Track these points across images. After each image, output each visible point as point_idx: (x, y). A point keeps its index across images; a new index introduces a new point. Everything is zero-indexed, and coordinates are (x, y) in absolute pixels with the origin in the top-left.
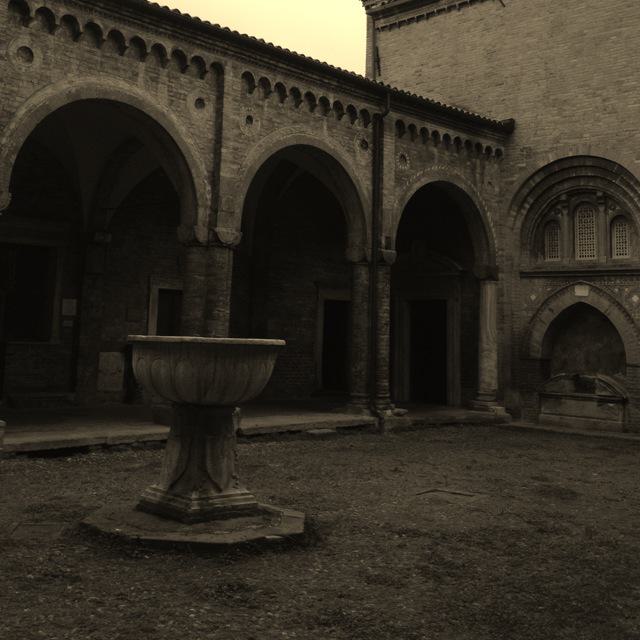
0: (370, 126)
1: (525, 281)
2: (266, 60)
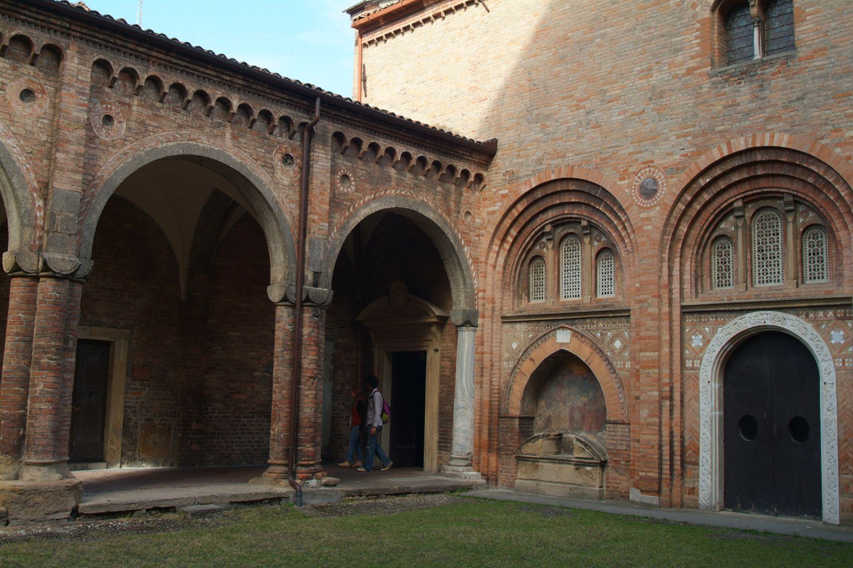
0: (297, 136)
1: (507, 326)
2: (130, 46)
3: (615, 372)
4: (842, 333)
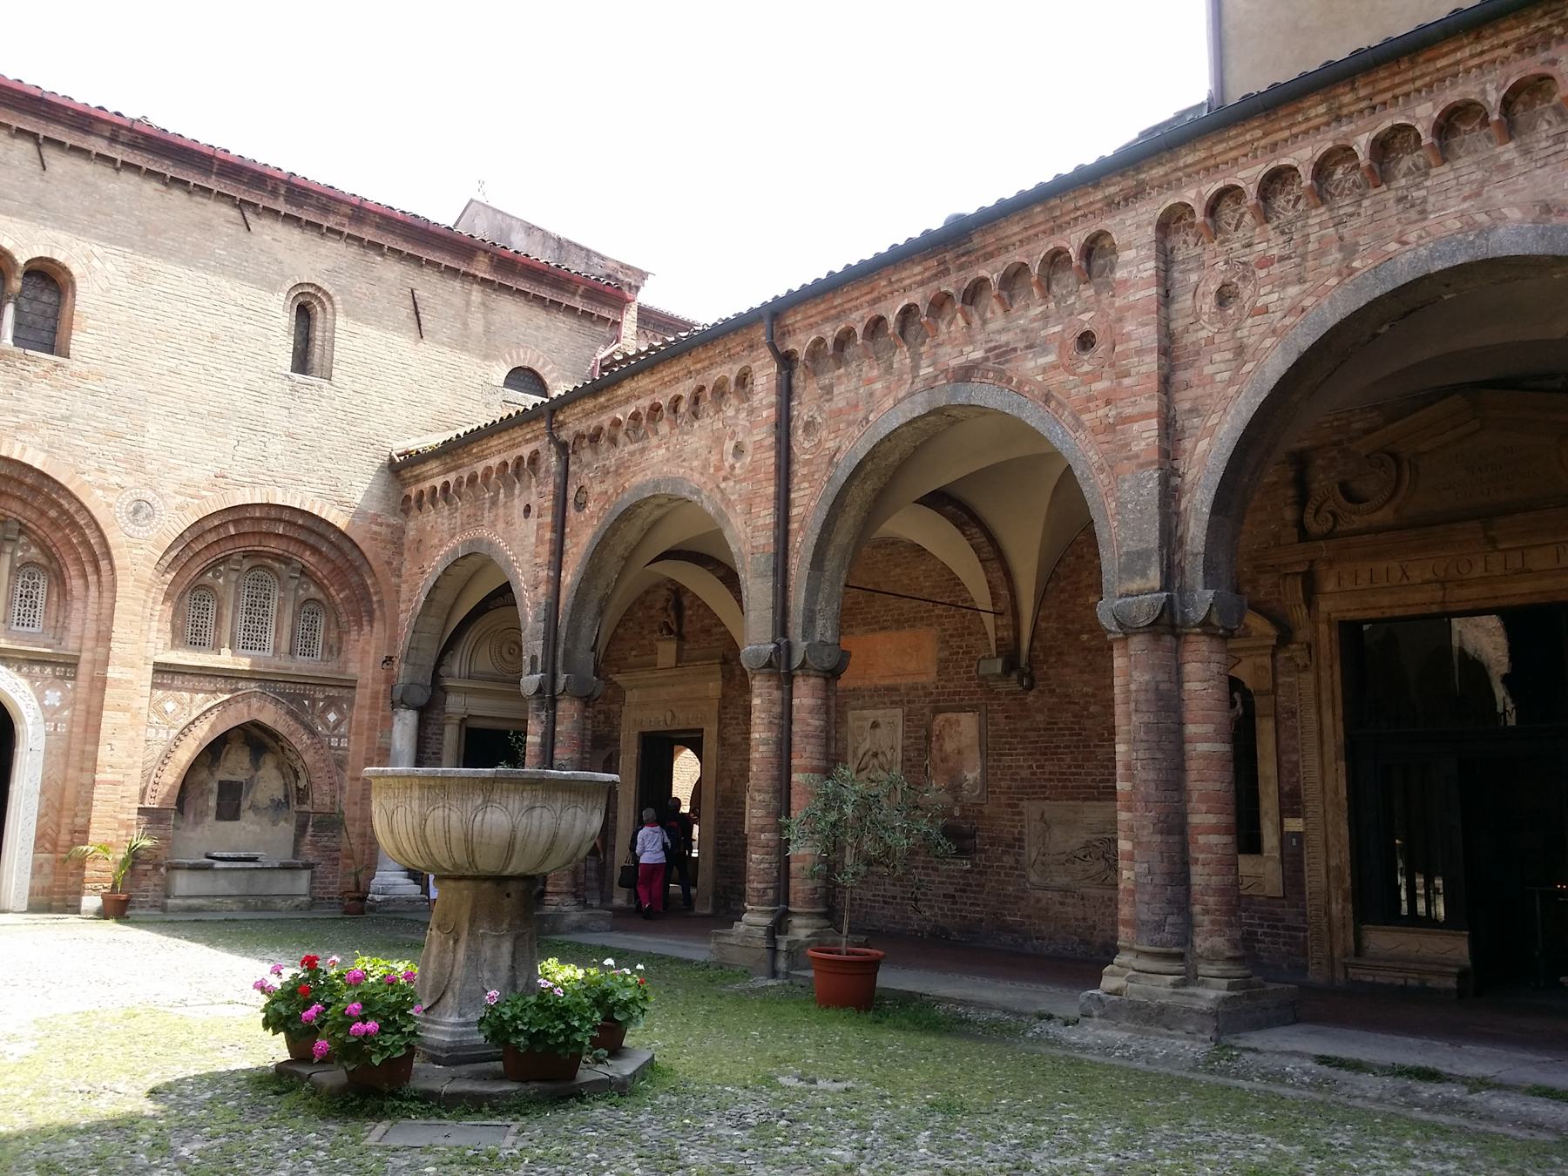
4: (59, 694)
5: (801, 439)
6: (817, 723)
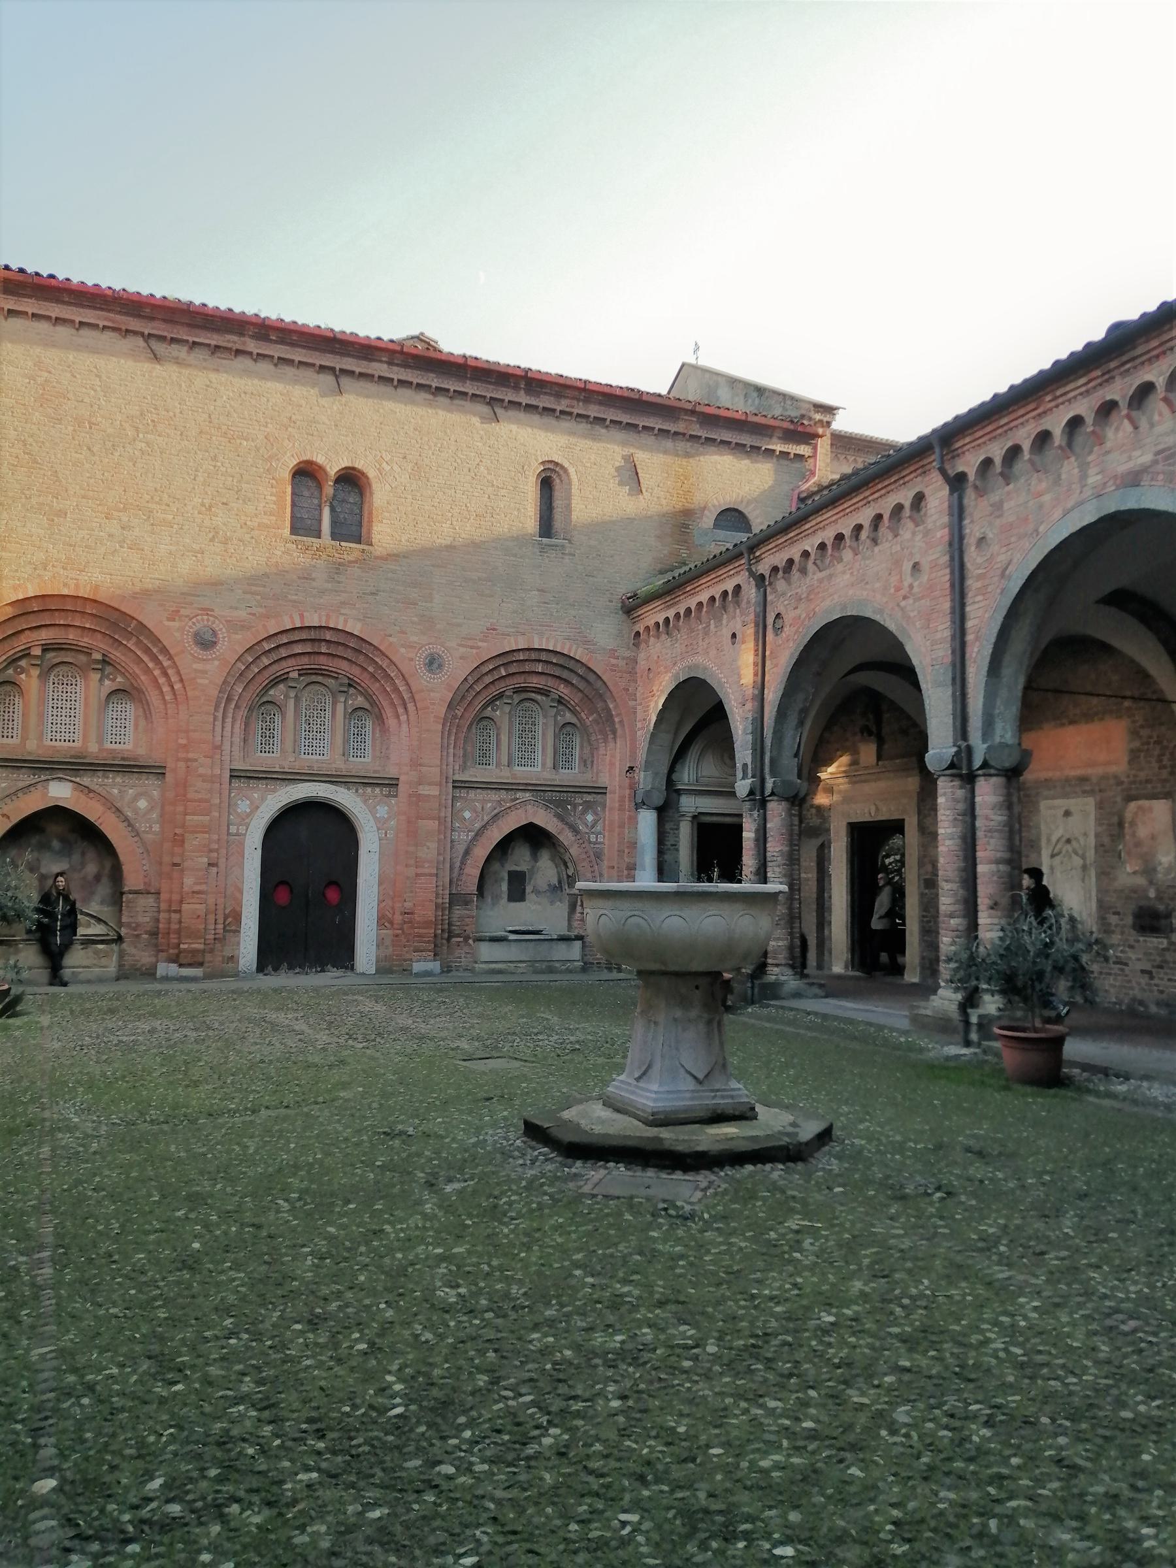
3: (138, 835)
5: (974, 555)
6: (1000, 818)
